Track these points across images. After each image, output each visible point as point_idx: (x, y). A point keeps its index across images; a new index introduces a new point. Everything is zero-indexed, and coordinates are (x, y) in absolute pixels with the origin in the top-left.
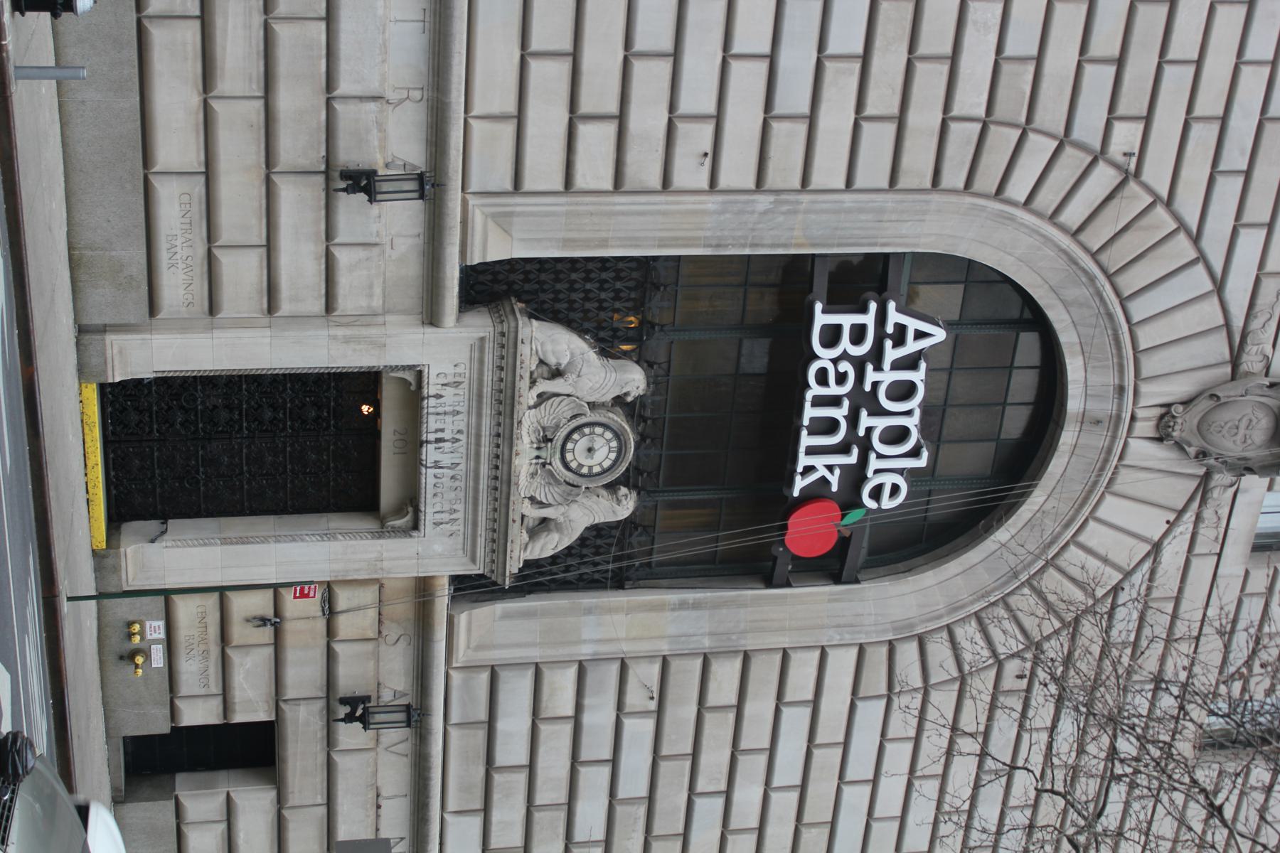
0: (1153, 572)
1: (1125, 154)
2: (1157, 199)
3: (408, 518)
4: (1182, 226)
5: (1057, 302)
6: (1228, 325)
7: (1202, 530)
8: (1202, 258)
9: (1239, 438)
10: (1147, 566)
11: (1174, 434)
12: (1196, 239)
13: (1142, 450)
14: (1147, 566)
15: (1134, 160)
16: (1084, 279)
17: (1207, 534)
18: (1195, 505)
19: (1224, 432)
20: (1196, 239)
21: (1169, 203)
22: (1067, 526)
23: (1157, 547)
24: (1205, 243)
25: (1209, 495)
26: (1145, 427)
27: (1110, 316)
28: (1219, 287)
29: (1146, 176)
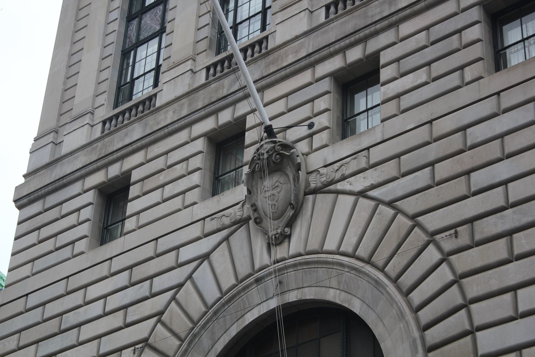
0: (373, 187)
1: (134, 353)
2: (159, 321)
4: (174, 298)
5: (213, 350)
6: (226, 239)
7: (347, 173)
8: (190, 277)
9: (275, 192)
10: (371, 193)
11: (279, 231)
12: (180, 286)
13: (295, 245)
14: (371, 193)
15: (137, 347)
16: (197, 340)
17: (353, 166)
18: (332, 187)
19: (274, 202)
20: (180, 286)
21: (161, 313)
22: (342, 265)
23: (362, 194)
24: (182, 280)
25: (325, 183)
27: (215, 313)
28: (206, 256)
29: (145, 335)
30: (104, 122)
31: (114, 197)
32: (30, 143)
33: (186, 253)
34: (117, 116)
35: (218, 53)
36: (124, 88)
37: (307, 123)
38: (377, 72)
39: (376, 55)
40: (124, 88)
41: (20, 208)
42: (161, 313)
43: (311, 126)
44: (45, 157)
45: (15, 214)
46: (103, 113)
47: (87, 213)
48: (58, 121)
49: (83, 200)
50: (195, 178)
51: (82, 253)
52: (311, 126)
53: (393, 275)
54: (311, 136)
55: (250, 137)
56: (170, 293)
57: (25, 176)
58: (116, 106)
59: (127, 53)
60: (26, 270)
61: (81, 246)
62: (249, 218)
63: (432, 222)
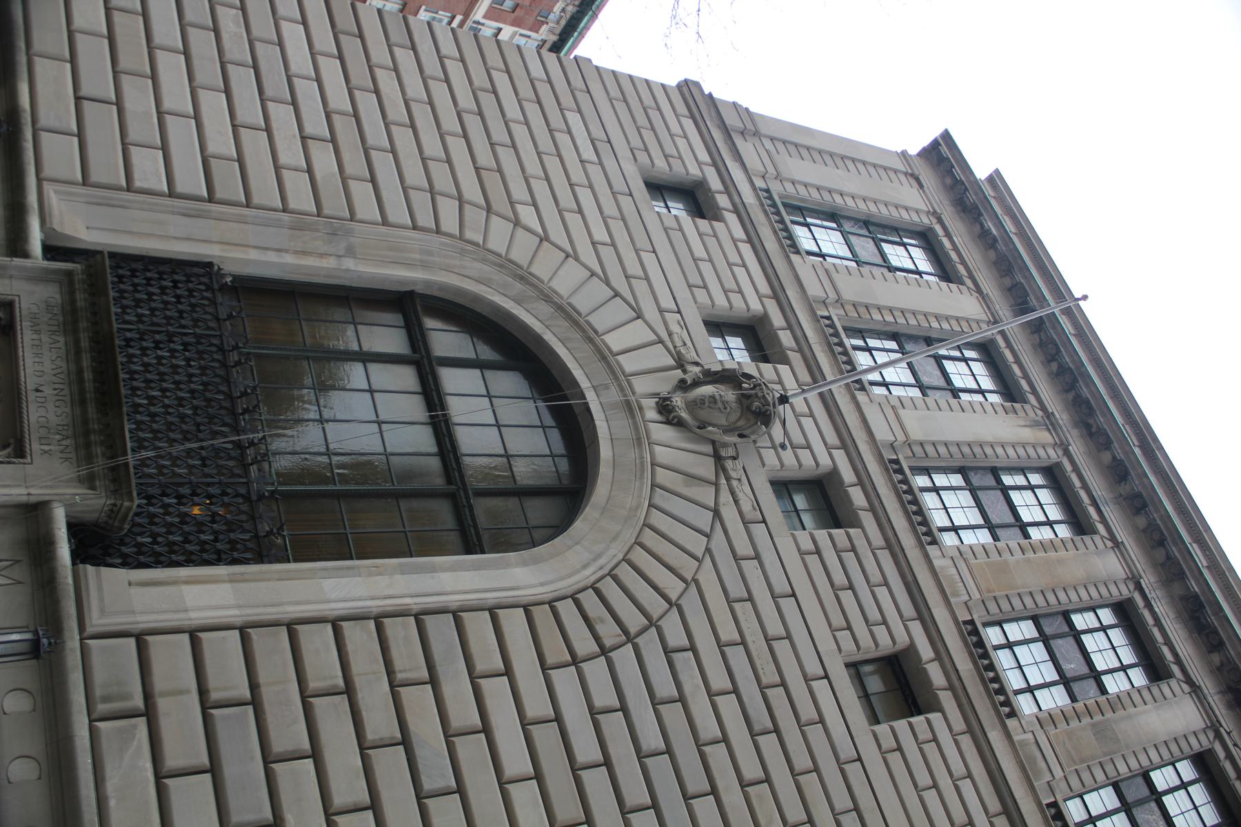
3: (8, 450)
4: (593, 274)
6: (661, 341)
8: (617, 294)
10: (718, 525)
12: (608, 283)
20: (608, 283)
21: (577, 259)
23: (716, 513)
24: (613, 284)
26: (652, 414)
28: (639, 316)
30: (767, 191)
31: (695, 199)
32: (744, 104)
33: (641, 287)
34: (774, 205)
35: (845, 329)
36: (802, 211)
37: (787, 443)
38: (838, 525)
39: (857, 524)
40: (802, 211)
41: (679, 86)
42: (577, 259)
43: (783, 446)
44: (731, 120)
45: (672, 81)
46: (776, 188)
47: (678, 168)
48: (766, 136)
49: (692, 163)
50: (720, 300)
51: (635, 159)
52: (783, 446)
53: (631, 556)
54: (774, 447)
55: (767, 368)
56: (598, 270)
57: (710, 94)
58: (785, 205)
59: (833, 216)
60: (614, 92)
61: (643, 158)
62: (685, 371)
63: (691, 604)
